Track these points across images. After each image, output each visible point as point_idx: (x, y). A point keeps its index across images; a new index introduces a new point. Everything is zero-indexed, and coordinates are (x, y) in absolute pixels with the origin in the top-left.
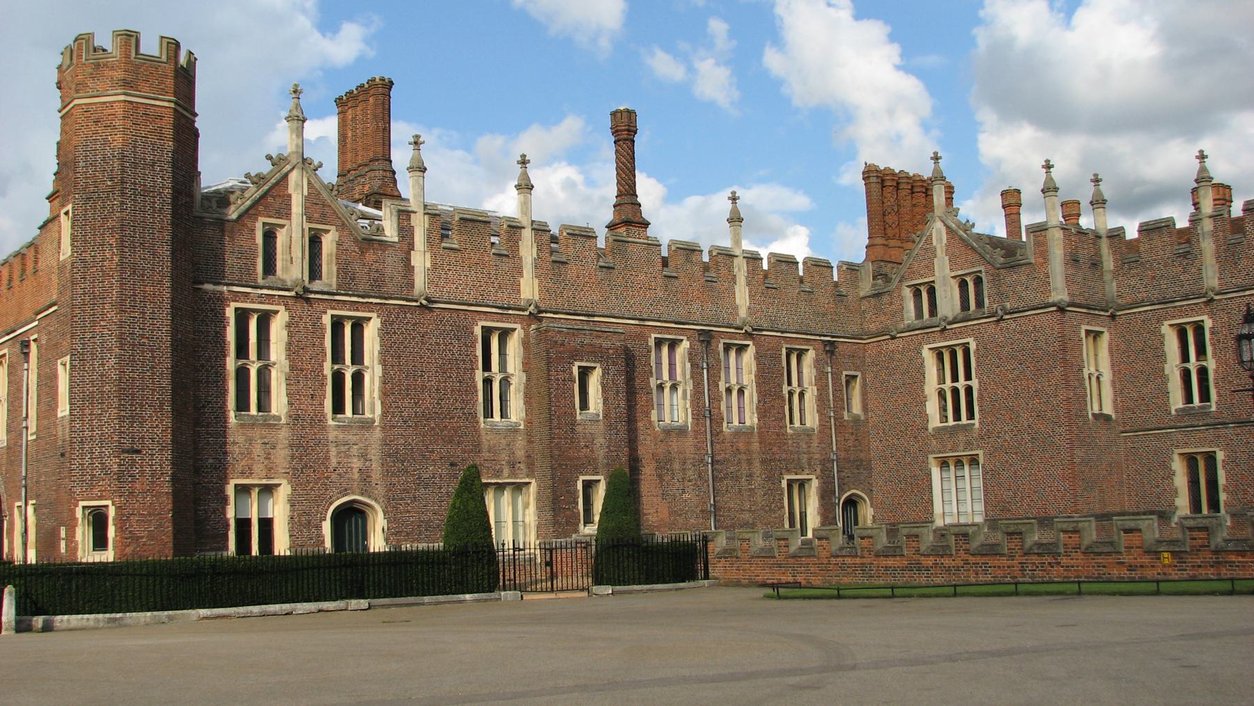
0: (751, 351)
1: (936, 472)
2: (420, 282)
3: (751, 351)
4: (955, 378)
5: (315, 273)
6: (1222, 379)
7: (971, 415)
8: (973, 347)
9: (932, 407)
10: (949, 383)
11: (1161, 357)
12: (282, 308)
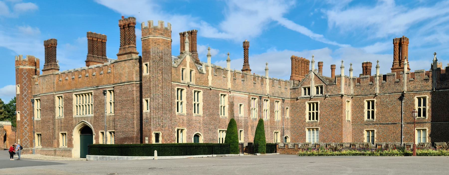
0: (269, 101)
1: (307, 131)
2: (210, 84)
3: (269, 101)
4: (313, 110)
5: (191, 81)
6: (378, 114)
7: (317, 119)
8: (319, 103)
9: (307, 116)
10: (312, 111)
11: (363, 107)
12: (185, 88)
